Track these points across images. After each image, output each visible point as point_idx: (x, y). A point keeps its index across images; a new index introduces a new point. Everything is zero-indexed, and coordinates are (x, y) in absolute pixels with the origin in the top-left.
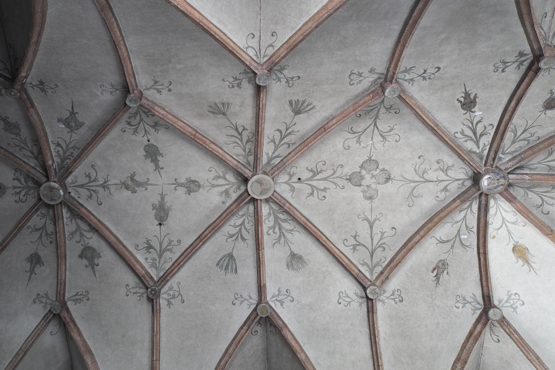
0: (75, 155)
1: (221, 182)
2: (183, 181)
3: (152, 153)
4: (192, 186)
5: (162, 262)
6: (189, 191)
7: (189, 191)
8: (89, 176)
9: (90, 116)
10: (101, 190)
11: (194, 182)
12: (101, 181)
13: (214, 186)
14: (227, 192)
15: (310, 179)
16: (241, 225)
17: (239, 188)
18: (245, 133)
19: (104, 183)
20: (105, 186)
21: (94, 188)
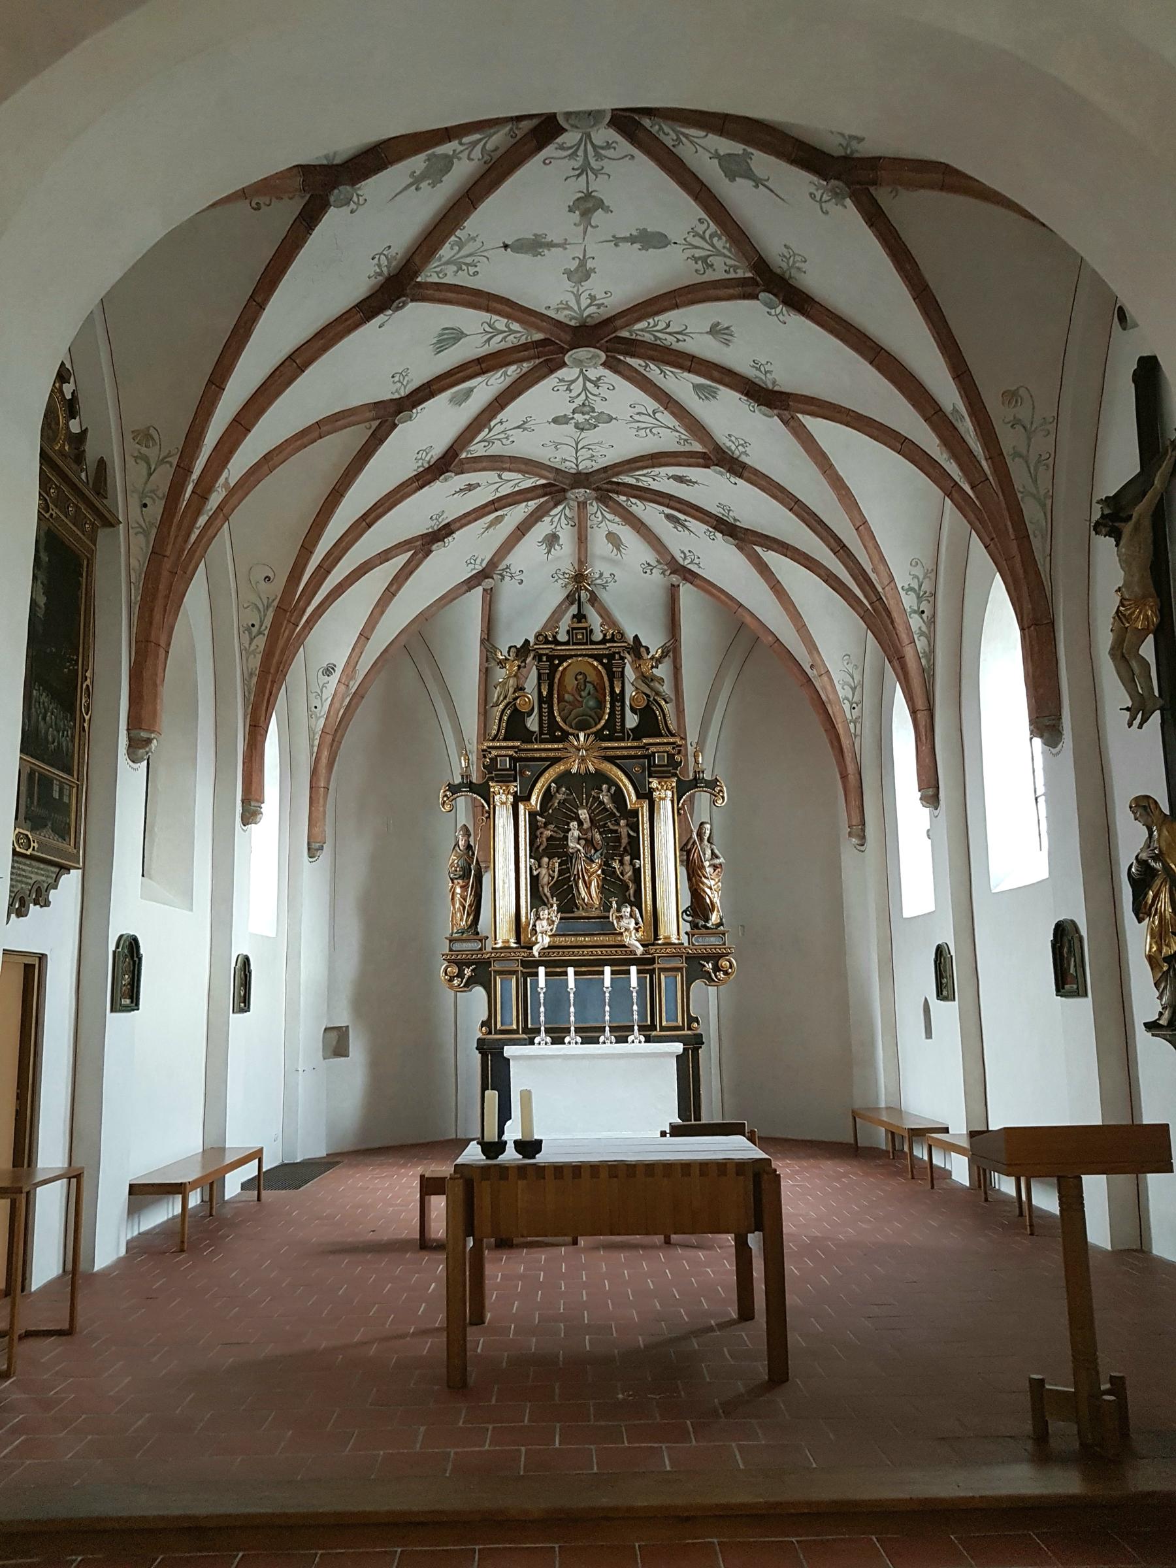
0: (662, 137)
1: (585, 302)
2: (590, 264)
3: (650, 240)
4: (581, 273)
5: (438, 269)
6: (569, 274)
7: (569, 274)
8: (608, 146)
9: (738, 195)
10: (578, 162)
11: (588, 277)
12: (594, 164)
13: (578, 297)
14: (569, 308)
15: (586, 378)
16: (510, 330)
17: (575, 318)
18: (671, 339)
19: (592, 169)
20: (584, 169)
21: (580, 153)
